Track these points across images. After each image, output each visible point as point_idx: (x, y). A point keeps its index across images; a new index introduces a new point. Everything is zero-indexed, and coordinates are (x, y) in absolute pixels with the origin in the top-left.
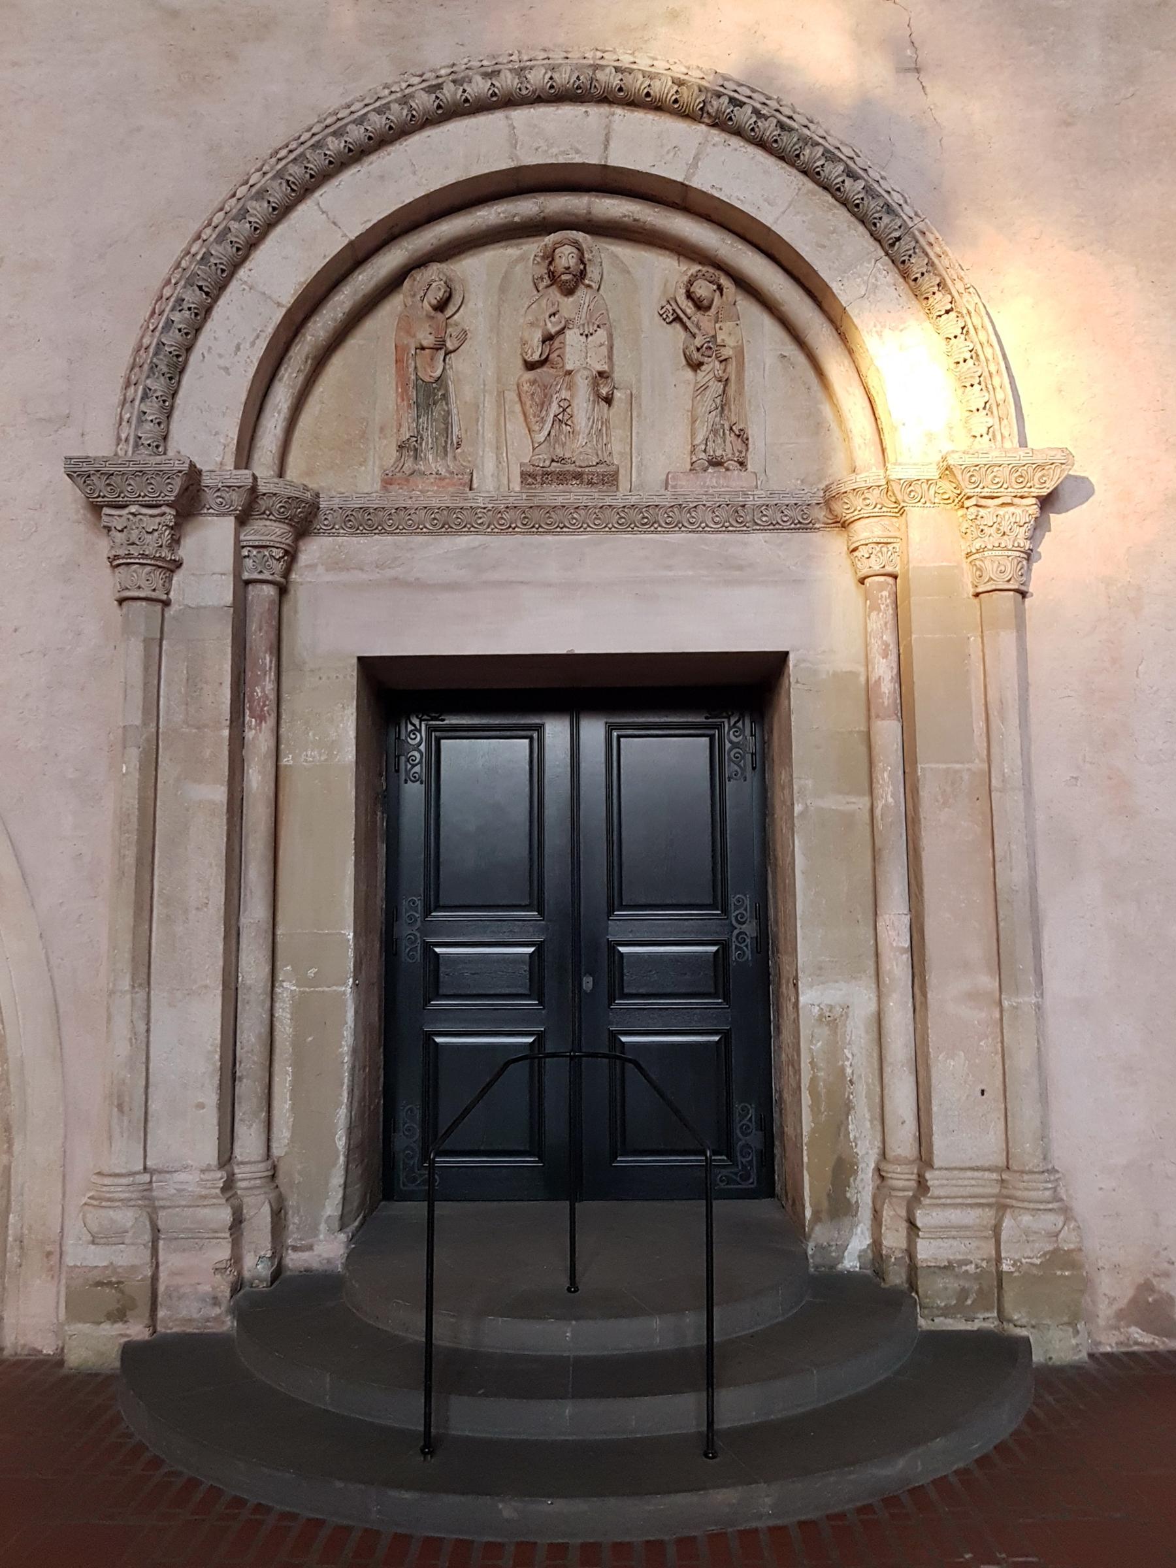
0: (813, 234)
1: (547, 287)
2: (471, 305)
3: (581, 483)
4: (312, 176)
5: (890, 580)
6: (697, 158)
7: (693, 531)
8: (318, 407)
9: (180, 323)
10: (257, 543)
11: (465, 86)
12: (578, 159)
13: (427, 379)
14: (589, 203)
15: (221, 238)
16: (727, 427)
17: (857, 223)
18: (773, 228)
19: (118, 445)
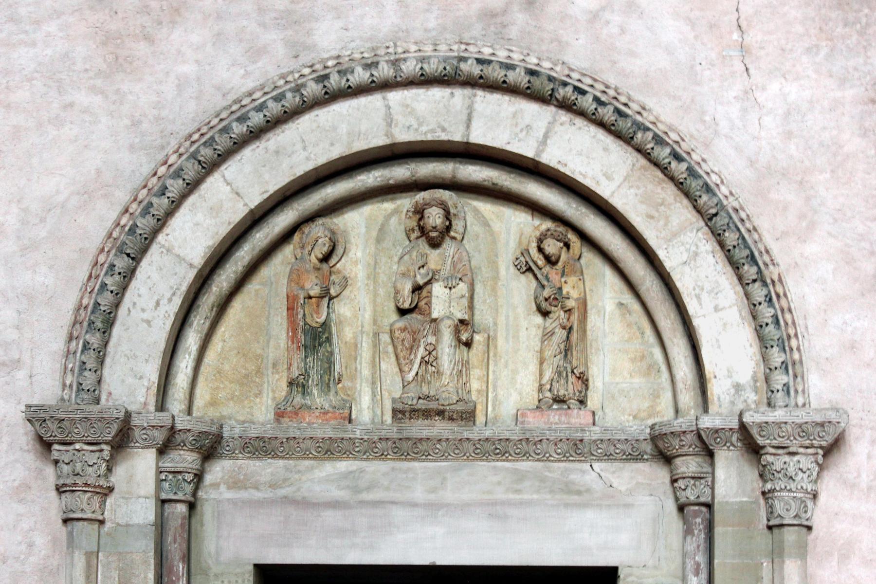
0: (644, 207)
1: (418, 238)
3: (443, 418)
4: (219, 155)
5: (704, 509)
6: (546, 136)
7: (538, 460)
8: (220, 345)
9: (112, 285)
10: (173, 470)
11: (350, 77)
12: (444, 137)
13: (314, 325)
14: (454, 171)
15: (145, 212)
16: (569, 370)
17: (682, 196)
18: (610, 201)
19: (63, 390)
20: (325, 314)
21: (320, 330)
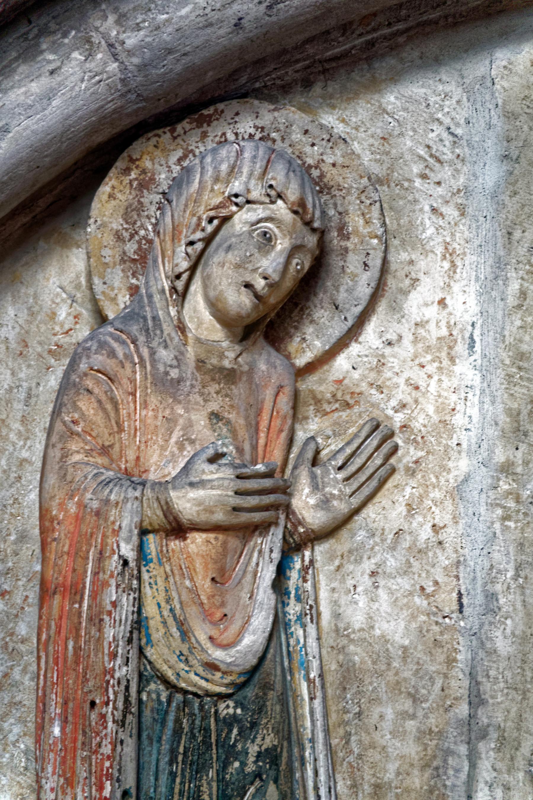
2: (418, 303)
13: (195, 680)
20: (261, 622)
21: (227, 708)
